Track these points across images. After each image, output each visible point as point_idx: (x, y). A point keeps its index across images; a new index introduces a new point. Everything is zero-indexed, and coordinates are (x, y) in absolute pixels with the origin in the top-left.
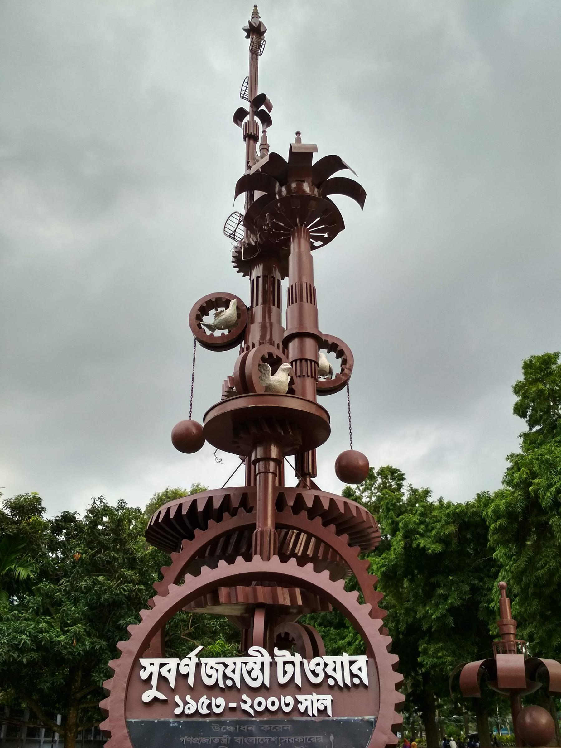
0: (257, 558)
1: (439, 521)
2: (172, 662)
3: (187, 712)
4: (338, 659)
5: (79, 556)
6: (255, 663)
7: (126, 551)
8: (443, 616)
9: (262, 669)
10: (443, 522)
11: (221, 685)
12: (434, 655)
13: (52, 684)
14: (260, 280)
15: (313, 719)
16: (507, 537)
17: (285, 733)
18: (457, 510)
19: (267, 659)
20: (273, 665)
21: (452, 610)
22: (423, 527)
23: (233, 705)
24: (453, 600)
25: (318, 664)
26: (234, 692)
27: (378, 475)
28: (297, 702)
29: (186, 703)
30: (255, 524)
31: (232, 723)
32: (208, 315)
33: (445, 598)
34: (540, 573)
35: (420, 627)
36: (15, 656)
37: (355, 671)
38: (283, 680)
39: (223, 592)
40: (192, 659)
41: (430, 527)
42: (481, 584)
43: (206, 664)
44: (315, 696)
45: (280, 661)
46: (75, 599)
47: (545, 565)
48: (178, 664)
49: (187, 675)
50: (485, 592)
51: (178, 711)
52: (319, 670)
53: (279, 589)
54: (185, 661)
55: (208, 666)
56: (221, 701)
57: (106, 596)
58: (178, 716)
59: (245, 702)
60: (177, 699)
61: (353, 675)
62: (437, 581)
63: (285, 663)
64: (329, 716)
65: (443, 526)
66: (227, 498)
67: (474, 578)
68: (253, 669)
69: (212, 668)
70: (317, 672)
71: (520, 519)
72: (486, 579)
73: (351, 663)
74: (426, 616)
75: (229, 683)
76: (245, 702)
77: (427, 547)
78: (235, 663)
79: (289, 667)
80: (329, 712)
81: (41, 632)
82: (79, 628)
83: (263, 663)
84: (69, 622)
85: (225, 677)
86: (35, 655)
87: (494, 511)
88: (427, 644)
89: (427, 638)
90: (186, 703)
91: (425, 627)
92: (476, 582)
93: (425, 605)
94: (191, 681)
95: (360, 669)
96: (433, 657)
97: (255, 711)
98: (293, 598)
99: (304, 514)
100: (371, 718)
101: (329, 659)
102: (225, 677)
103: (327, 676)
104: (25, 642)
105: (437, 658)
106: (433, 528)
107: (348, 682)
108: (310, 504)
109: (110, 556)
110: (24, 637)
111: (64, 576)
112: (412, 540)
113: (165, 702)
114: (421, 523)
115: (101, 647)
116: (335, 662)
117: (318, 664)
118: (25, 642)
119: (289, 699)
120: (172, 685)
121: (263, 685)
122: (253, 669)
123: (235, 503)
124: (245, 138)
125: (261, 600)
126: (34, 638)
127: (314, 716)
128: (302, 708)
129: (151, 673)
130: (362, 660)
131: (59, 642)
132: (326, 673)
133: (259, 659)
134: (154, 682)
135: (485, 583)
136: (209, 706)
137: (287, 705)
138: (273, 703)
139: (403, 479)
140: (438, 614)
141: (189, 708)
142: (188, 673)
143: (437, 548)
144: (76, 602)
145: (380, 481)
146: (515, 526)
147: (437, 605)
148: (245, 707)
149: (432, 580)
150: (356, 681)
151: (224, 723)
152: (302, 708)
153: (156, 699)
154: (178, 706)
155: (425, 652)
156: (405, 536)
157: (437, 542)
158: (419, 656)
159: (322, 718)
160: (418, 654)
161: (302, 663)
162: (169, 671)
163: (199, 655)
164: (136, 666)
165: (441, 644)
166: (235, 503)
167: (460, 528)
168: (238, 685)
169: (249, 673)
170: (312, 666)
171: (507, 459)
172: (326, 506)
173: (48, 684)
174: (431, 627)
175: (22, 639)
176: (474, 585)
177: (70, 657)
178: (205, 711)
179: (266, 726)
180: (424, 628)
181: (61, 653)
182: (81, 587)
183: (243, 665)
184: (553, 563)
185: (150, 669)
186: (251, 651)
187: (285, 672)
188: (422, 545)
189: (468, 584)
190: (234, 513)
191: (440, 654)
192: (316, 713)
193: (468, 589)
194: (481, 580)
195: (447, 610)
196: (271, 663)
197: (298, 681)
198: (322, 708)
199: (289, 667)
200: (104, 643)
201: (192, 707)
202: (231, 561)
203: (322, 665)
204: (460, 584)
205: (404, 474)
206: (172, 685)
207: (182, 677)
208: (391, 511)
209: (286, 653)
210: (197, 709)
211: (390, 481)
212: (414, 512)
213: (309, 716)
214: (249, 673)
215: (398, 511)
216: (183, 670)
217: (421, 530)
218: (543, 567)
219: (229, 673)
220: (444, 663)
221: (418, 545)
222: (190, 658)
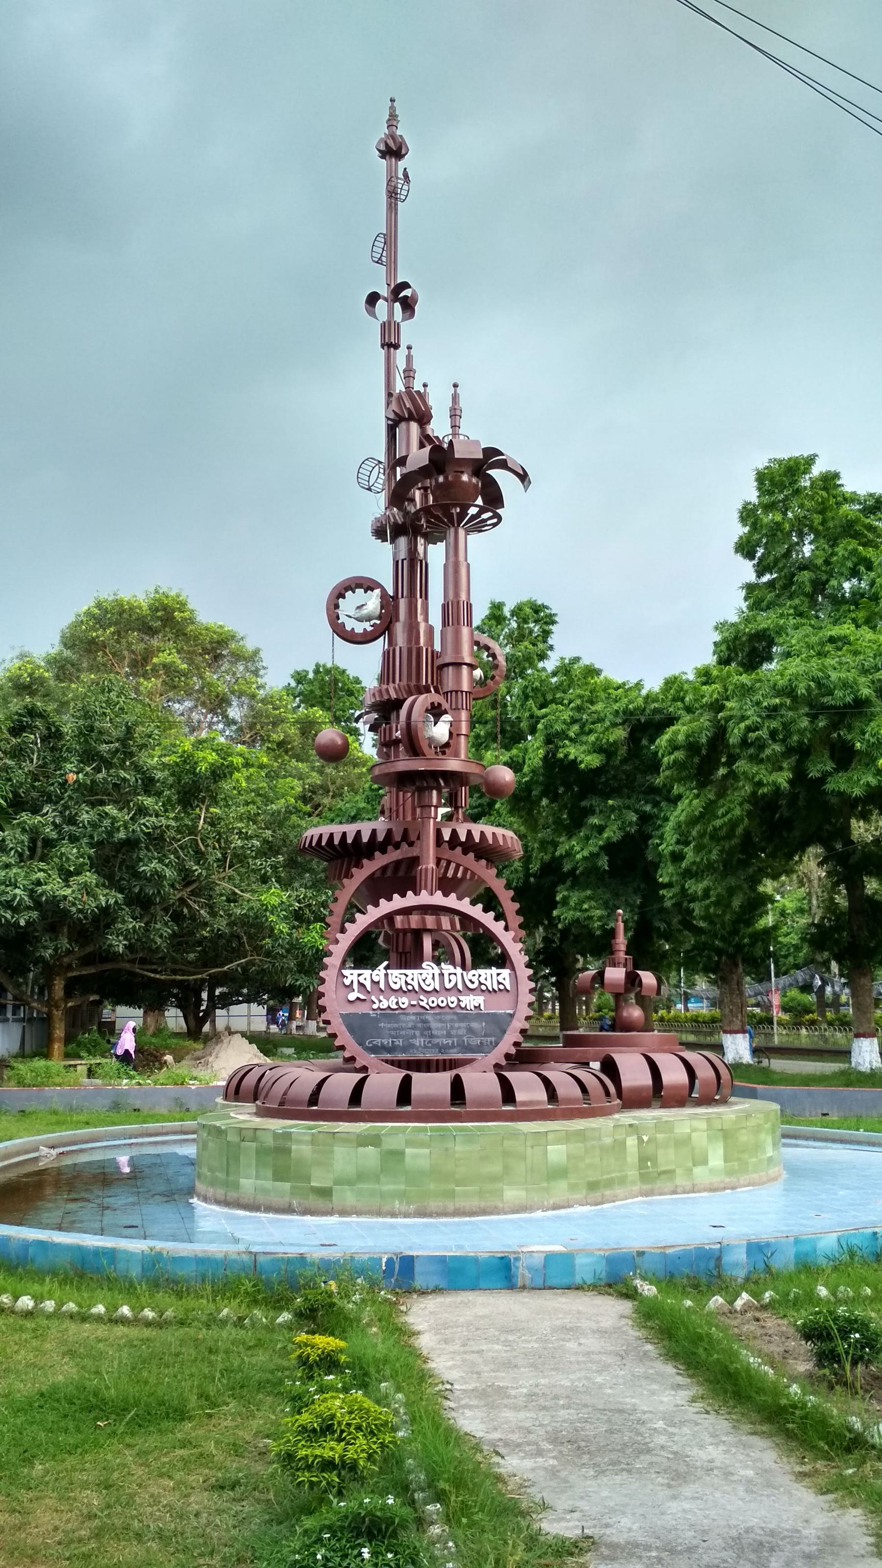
0: (423, 892)
1: (600, 720)
2: (367, 973)
4: (488, 971)
5: (75, 777)
7: (137, 768)
8: (593, 856)
9: (433, 978)
10: (607, 723)
11: (404, 989)
12: (578, 907)
13: (56, 950)
16: (684, 774)
18: (631, 706)
19: (437, 971)
20: (442, 975)
21: (609, 848)
22: (576, 728)
24: (612, 833)
26: (413, 993)
27: (512, 615)
28: (459, 1001)
29: (380, 1001)
31: (414, 1014)
32: (344, 597)
33: (601, 829)
34: (718, 823)
35: (560, 867)
36: (8, 916)
37: (501, 981)
38: (448, 986)
39: (399, 919)
40: (380, 971)
41: (587, 729)
42: (655, 810)
44: (472, 997)
46: (70, 836)
47: (727, 813)
50: (659, 822)
51: (375, 1006)
52: (475, 979)
53: (442, 918)
54: (376, 972)
57: (122, 835)
61: (499, 983)
62: (591, 805)
65: (607, 729)
66: (389, 832)
67: (646, 802)
71: (704, 752)
72: (663, 804)
73: (498, 974)
74: (569, 854)
75: (410, 988)
77: (579, 759)
80: (482, 1007)
81: (39, 883)
82: (90, 877)
84: (72, 869)
86: (35, 914)
87: (670, 741)
88: (567, 890)
89: (569, 883)
90: (380, 1001)
91: (567, 867)
92: (648, 808)
93: (570, 838)
94: (382, 986)
96: (575, 909)
99: (459, 850)
100: (511, 1012)
101: (481, 971)
103: (480, 984)
104: (21, 899)
105: (581, 910)
106: (591, 731)
108: (463, 838)
109: (118, 776)
110: (17, 891)
111: (47, 802)
112: (557, 748)
114: (574, 721)
115: (116, 902)
118: (21, 899)
119: (454, 999)
120: (369, 988)
121: (435, 990)
123: (397, 837)
124: (383, 346)
125: (429, 927)
126: (31, 893)
130: (506, 972)
131: (65, 897)
133: (431, 972)
135: (661, 810)
136: (397, 1003)
139: (553, 622)
140: (586, 853)
143: (593, 761)
144: (73, 839)
145: (514, 625)
146: (696, 760)
147: (587, 838)
148: (422, 1003)
149: (584, 803)
150: (501, 987)
152: (463, 1005)
155: (565, 901)
156: (548, 740)
157: (595, 751)
158: (555, 908)
160: (554, 905)
163: (387, 968)
165: (589, 892)
166: (397, 837)
167: (631, 733)
168: (417, 989)
171: (716, 628)
173: (50, 951)
174: (575, 869)
175: (15, 896)
176: (645, 812)
177: (80, 916)
178: (394, 1006)
180: (565, 870)
181: (70, 911)
182: (83, 822)
184: (737, 812)
186: (424, 965)
188: (572, 757)
189: (636, 811)
190: (397, 846)
191: (585, 906)
193: (635, 819)
194: (656, 804)
195: (601, 848)
197: (460, 986)
199: (453, 977)
200: (120, 896)
201: (384, 1004)
202: (403, 895)
204: (624, 811)
205: (555, 615)
208: (531, 701)
211: (532, 625)
212: (566, 702)
215: (542, 699)
216: (376, 979)
217: (572, 734)
218: (723, 815)
219: (409, 981)
220: (590, 918)
221: (566, 756)
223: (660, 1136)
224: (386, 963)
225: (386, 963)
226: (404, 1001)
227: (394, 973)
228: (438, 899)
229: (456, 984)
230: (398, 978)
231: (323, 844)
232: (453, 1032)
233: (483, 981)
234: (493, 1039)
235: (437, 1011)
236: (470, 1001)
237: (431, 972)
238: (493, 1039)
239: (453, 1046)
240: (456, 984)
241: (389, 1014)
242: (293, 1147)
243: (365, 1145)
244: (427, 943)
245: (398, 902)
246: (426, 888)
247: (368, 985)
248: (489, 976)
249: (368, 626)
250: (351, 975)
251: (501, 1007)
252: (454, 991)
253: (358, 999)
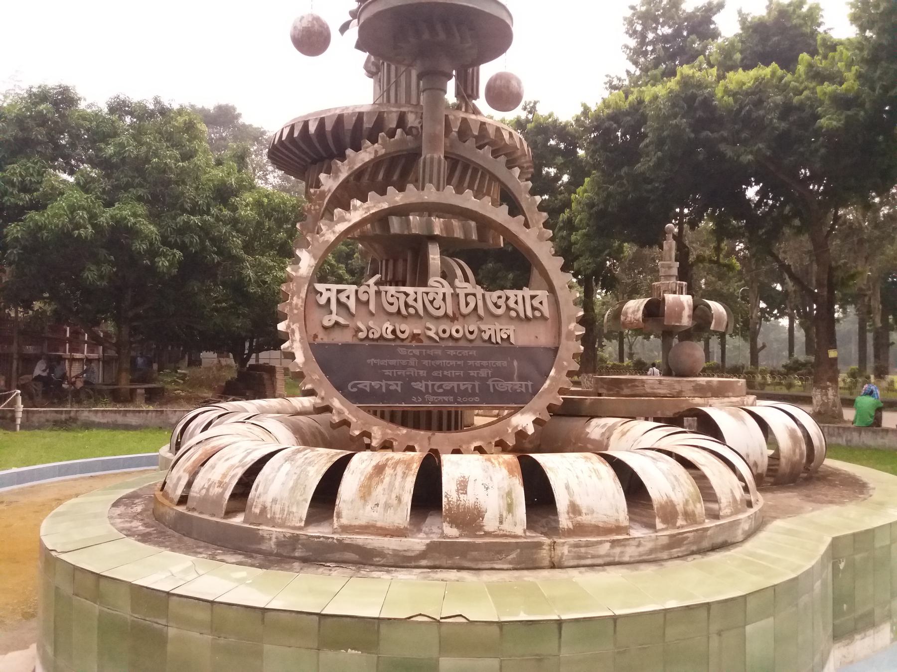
3: (371, 336)
4: (520, 293)
6: (437, 293)
9: (444, 299)
11: (404, 311)
15: (497, 346)
17: (471, 357)
19: (448, 290)
20: (456, 296)
25: (500, 297)
30: (420, 148)
43: (386, 292)
44: (498, 327)
48: (357, 291)
49: (367, 303)
52: (501, 302)
54: (363, 288)
55: (389, 295)
56: (404, 327)
58: (362, 340)
59: (430, 329)
61: (534, 309)
63: (467, 295)
64: (512, 344)
68: (434, 299)
69: (392, 296)
70: (499, 304)
73: (533, 297)
76: (430, 329)
78: (416, 293)
79: (471, 299)
83: (444, 294)
85: (407, 305)
94: (372, 307)
95: (541, 303)
97: (440, 338)
98: (466, 231)
101: (511, 293)
102: (407, 305)
103: (509, 308)
107: (529, 313)
113: (346, 326)
116: (516, 296)
117: (500, 297)
121: (446, 315)
122: (434, 299)
125: (437, 232)
127: (497, 343)
128: (486, 337)
129: (329, 300)
132: (508, 307)
134: (334, 306)
137: (471, 333)
138: (457, 331)
141: (373, 333)
142: (368, 300)
150: (537, 314)
151: (411, 347)
153: (337, 323)
154: (362, 331)
159: (505, 344)
161: (483, 295)
162: (348, 297)
163: (376, 284)
168: (421, 312)
169: (431, 302)
170: (495, 300)
178: (390, 336)
179: (452, 351)
183: (425, 295)
187: (467, 304)
192: (499, 341)
196: (452, 294)
198: (505, 336)
199: (471, 299)
203: (504, 299)
210: (382, 334)
213: (493, 343)
214: (431, 302)
216: (364, 298)
219: (410, 301)
222: (369, 286)
223: (858, 557)
224: (378, 276)
228: (449, 196)
231: (296, 134)
232: (472, 373)
233: (511, 303)
234: (530, 383)
235: (451, 343)
238: (530, 383)
239: (473, 394)
241: (379, 346)
242: (172, 632)
243: (337, 645)
244: (435, 256)
245: (395, 197)
246: (431, 182)
247: (352, 303)
250: (327, 291)
252: (474, 318)
253: (337, 323)
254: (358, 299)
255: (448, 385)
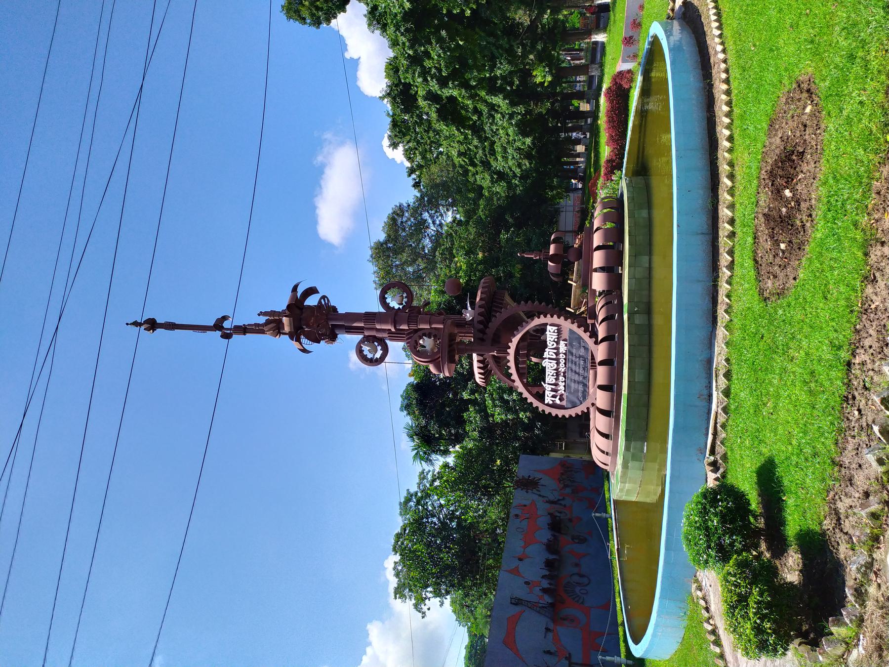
2: (547, 393)
4: (548, 336)
14: (347, 330)
20: (549, 359)
23: (562, 374)
37: (552, 331)
38: (554, 357)
45: (548, 356)
51: (563, 392)
52: (552, 343)
54: (546, 388)
60: (559, 392)
61: (554, 332)
73: (550, 331)
75: (555, 374)
79: (550, 353)
94: (554, 387)
108: (482, 326)
119: (561, 355)
123: (481, 358)
130: (549, 328)
133: (547, 363)
134: (553, 399)
136: (562, 382)
150: (556, 331)
152: (564, 352)
163: (545, 383)
164: (548, 405)
172: (482, 318)
178: (564, 384)
185: (549, 400)
186: (544, 366)
197: (555, 351)
199: (550, 353)
206: (554, 393)
207: (553, 390)
209: (545, 353)
216: (550, 389)
219: (552, 374)
224: (542, 383)
225: (542, 383)
226: (561, 378)
227: (547, 380)
229: (554, 353)
230: (550, 378)
233: (552, 340)
236: (563, 348)
237: (547, 363)
240: (554, 353)
248: (550, 335)
249: (379, 348)
250: (548, 400)
251: (565, 334)
254: (551, 391)
255: (581, 369)
